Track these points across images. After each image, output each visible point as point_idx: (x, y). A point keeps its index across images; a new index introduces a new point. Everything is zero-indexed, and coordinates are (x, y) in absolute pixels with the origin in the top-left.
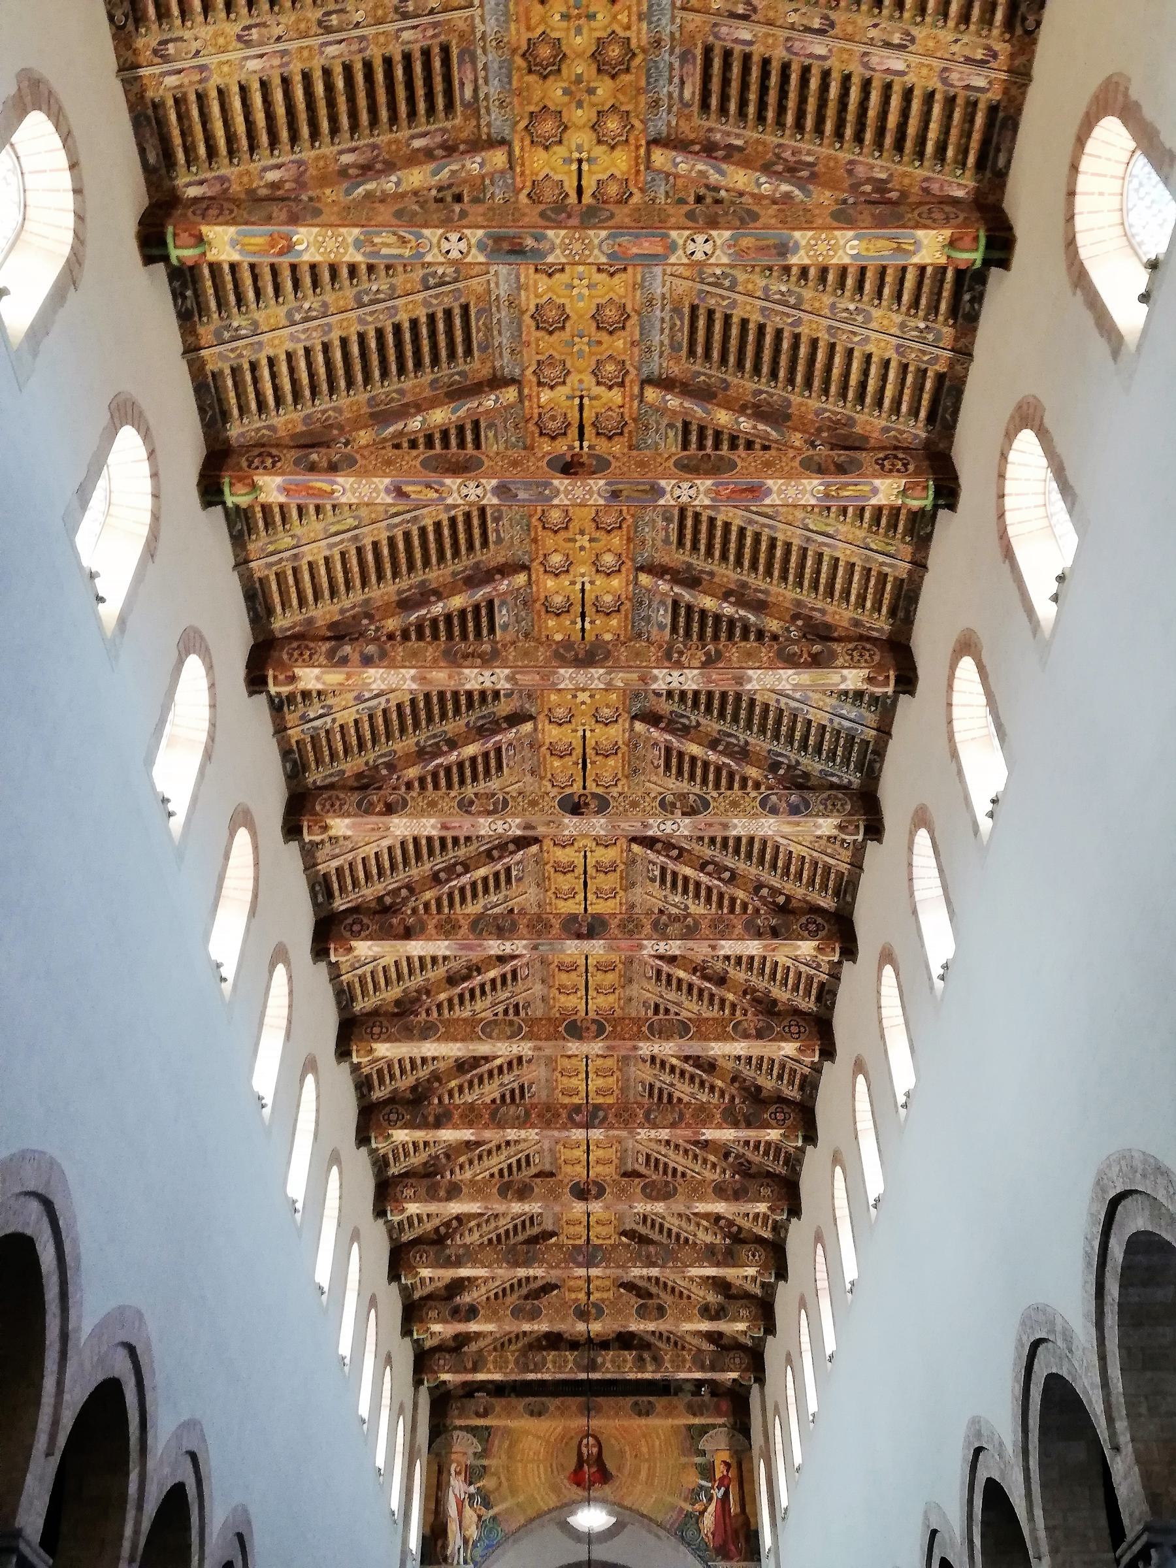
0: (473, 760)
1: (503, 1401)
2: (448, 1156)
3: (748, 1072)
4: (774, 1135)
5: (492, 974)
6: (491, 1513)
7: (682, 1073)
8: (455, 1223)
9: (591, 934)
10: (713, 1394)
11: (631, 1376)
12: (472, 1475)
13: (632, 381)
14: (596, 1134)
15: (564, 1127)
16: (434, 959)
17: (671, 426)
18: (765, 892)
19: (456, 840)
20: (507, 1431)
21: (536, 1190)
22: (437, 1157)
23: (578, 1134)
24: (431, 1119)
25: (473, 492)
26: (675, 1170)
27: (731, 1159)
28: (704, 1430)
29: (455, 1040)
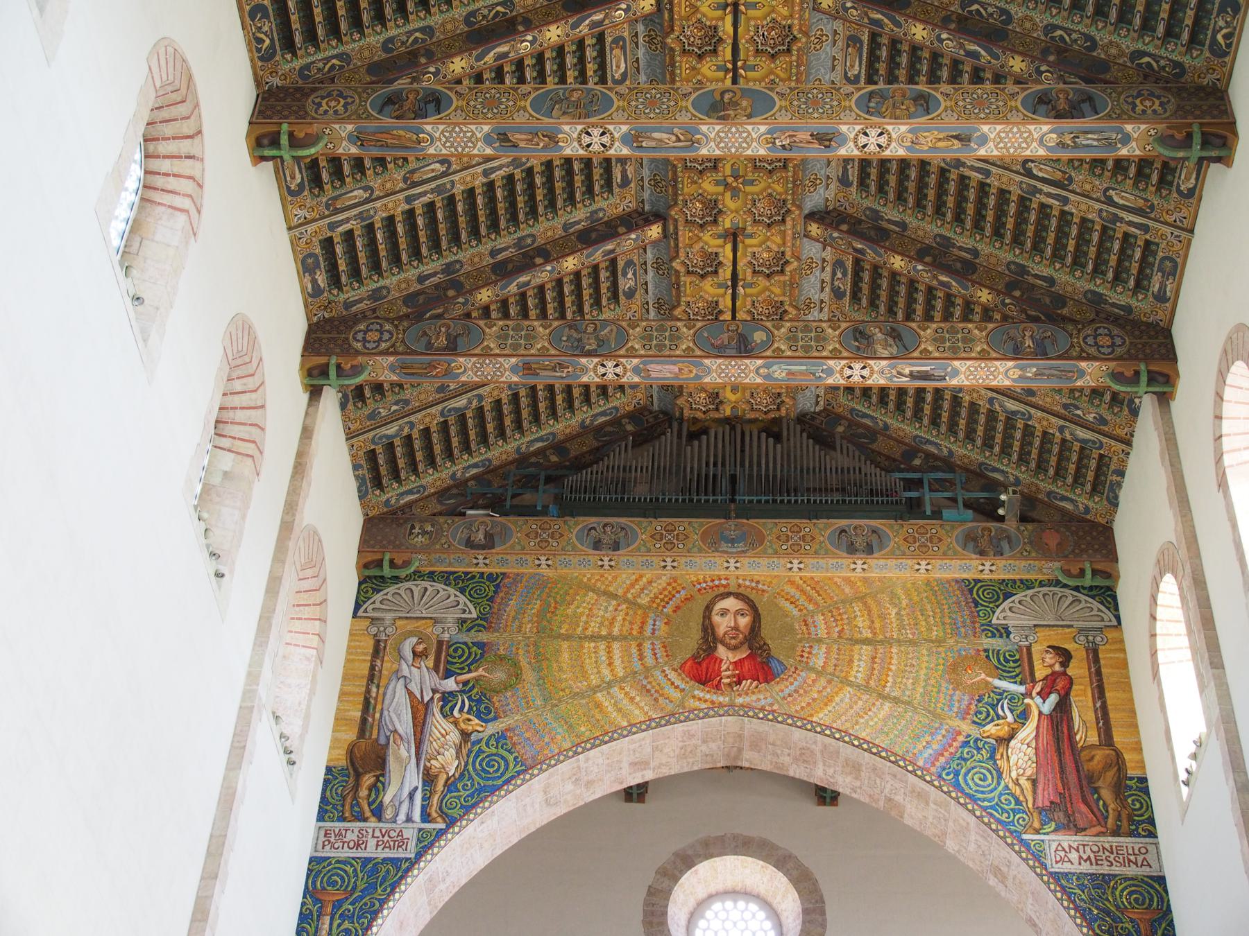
6: (492, 728)
17: (839, 264)
20: (542, 584)
28: (1003, 590)
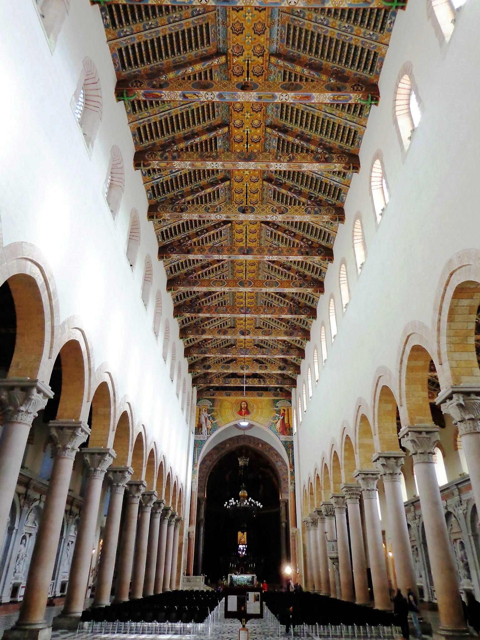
0: (210, 194)
1: (219, 392)
2: (201, 321)
3: (297, 298)
4: (303, 317)
5: (215, 266)
6: (215, 422)
7: (275, 298)
8: (204, 341)
9: (247, 254)
10: (281, 391)
11: (257, 386)
12: (209, 412)
13: (266, 54)
14: (248, 316)
15: (238, 313)
16: (197, 260)
17: (280, 72)
18: (305, 240)
19: (204, 221)
20: (220, 400)
21: (229, 332)
22: (199, 322)
23: (242, 316)
24: (196, 310)
25: (210, 97)
26: (272, 327)
27: (289, 324)
29: (204, 286)
